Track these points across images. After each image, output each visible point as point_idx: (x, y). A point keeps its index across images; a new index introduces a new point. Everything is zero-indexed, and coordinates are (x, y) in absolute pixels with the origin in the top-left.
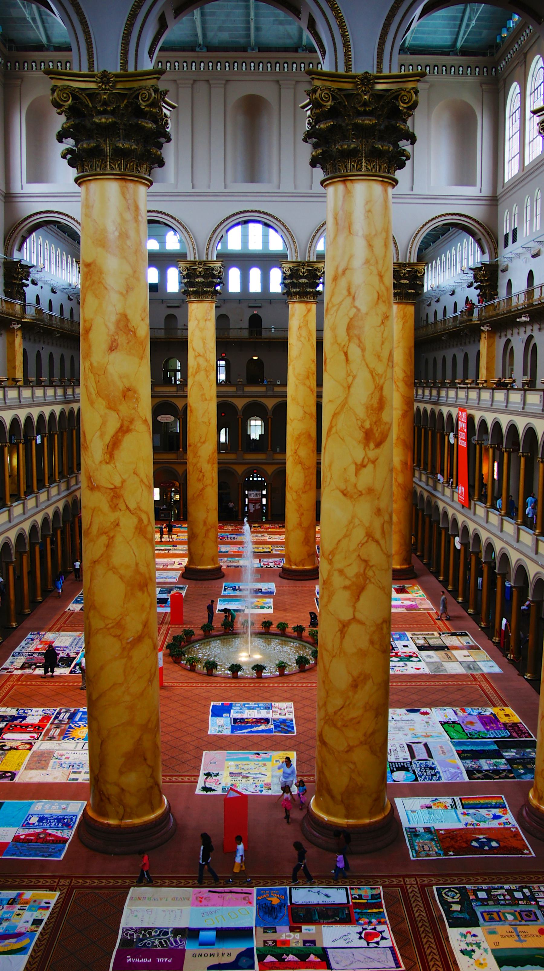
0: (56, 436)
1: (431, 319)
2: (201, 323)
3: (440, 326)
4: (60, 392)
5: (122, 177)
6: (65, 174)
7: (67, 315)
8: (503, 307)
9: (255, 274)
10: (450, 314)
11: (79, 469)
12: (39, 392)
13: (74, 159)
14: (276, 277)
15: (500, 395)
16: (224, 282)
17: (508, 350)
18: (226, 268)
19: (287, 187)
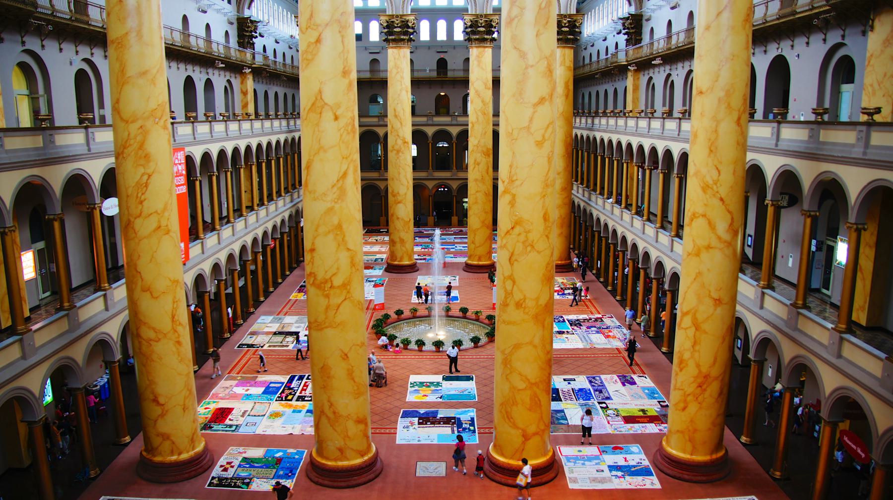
0: (264, 164)
1: (587, 61)
2: (399, 65)
3: (594, 67)
4: (284, 123)
7: (288, 61)
8: (645, 52)
9: (442, 25)
10: (603, 56)
11: (300, 185)
12: (267, 124)
14: (459, 27)
15: (643, 123)
16: (416, 32)
17: (650, 86)
18: (418, 20)
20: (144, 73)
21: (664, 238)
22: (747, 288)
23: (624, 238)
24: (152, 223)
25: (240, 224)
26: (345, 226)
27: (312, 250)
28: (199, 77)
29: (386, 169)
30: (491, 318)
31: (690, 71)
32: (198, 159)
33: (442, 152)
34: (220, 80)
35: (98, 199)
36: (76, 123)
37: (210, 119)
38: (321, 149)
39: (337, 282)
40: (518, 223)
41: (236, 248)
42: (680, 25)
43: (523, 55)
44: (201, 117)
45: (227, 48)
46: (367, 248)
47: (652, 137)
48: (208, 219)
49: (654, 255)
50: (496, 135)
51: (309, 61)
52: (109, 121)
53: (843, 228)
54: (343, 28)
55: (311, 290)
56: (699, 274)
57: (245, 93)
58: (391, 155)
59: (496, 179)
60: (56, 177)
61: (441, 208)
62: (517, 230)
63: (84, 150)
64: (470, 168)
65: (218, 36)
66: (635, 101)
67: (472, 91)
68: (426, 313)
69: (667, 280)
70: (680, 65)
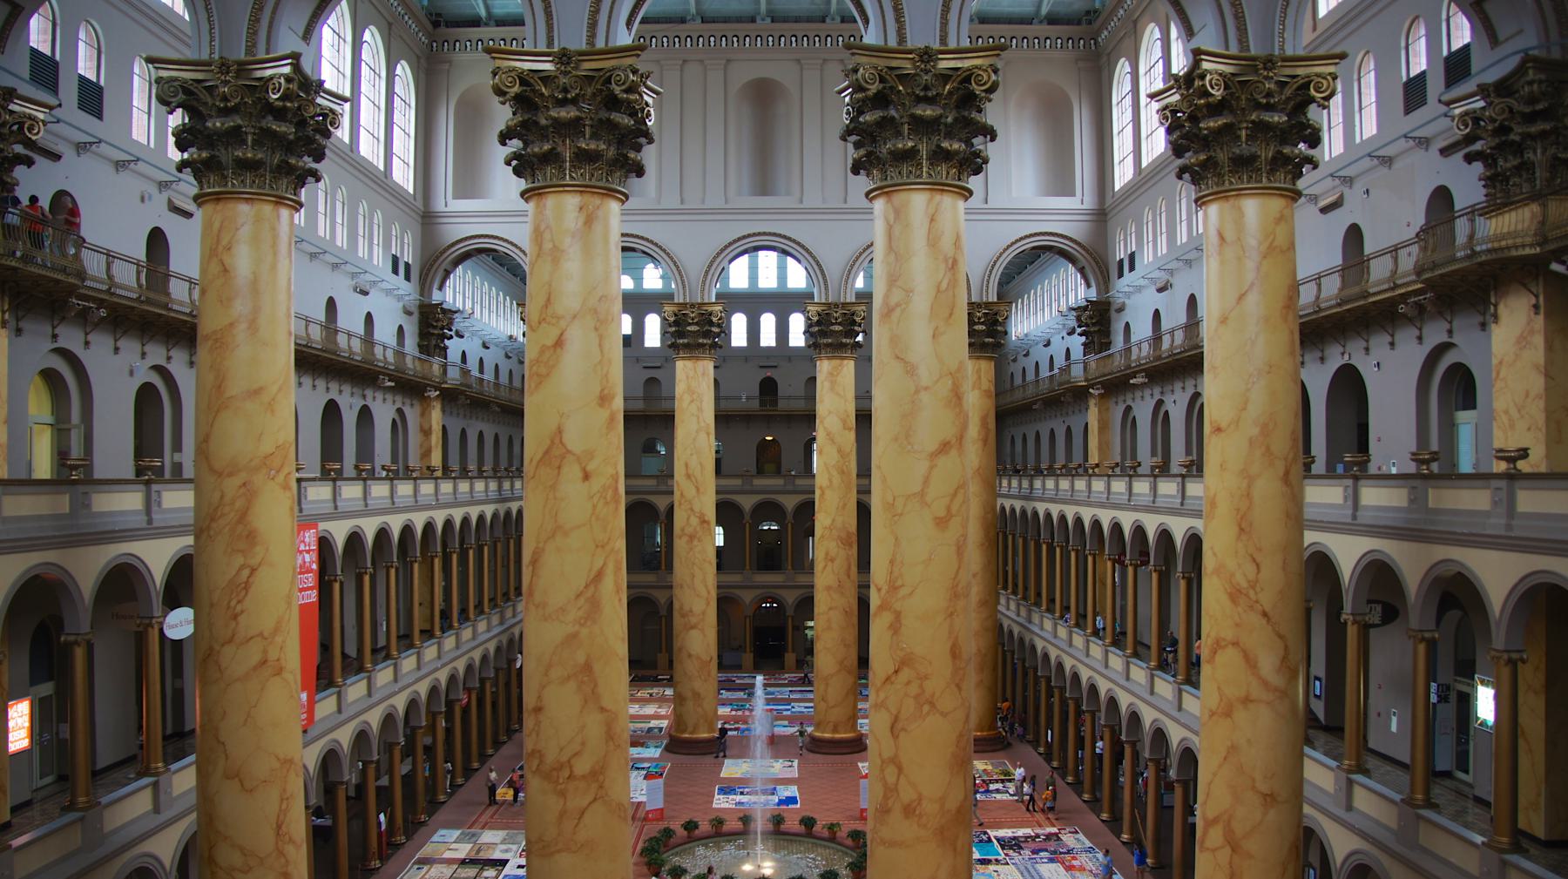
0: (455, 557)
1: (1018, 381)
2: (694, 388)
3: (1030, 391)
4: (493, 485)
5: (584, 189)
6: (505, 186)
7: (504, 379)
8: (1118, 362)
9: (768, 322)
10: (1045, 372)
12: (464, 486)
13: (522, 165)
14: (797, 323)
15: (1119, 486)
16: (726, 332)
17: (1129, 422)
19: (812, 200)
20: (256, 392)
21: (1165, 687)
22: (1320, 773)
23: (1093, 689)
24: (253, 654)
25: (408, 663)
26: (597, 667)
27: (538, 710)
28: (349, 402)
29: (670, 567)
30: (857, 836)
31: (1197, 396)
32: (340, 542)
33: (768, 538)
34: (384, 411)
35: (157, 612)
36: (131, 475)
37: (365, 475)
38: (558, 530)
39: (582, 766)
40: (905, 662)
41: (400, 703)
42: (1175, 317)
43: (910, 370)
44: (349, 470)
45: (400, 354)
46: (634, 709)
47: (1136, 509)
48: (352, 651)
49: (1148, 716)
50: (864, 512)
51: (541, 379)
52: (188, 472)
53: (1482, 660)
54: (602, 323)
55: (534, 784)
56: (1233, 749)
57: (427, 433)
58: (680, 544)
59: (864, 587)
60: (86, 569)
61: (767, 639)
62: (906, 673)
63: (141, 521)
64: (818, 567)
65: (385, 333)
66: (1104, 447)
67: (820, 434)
68: (739, 826)
69: (1174, 760)
70: (1178, 385)
